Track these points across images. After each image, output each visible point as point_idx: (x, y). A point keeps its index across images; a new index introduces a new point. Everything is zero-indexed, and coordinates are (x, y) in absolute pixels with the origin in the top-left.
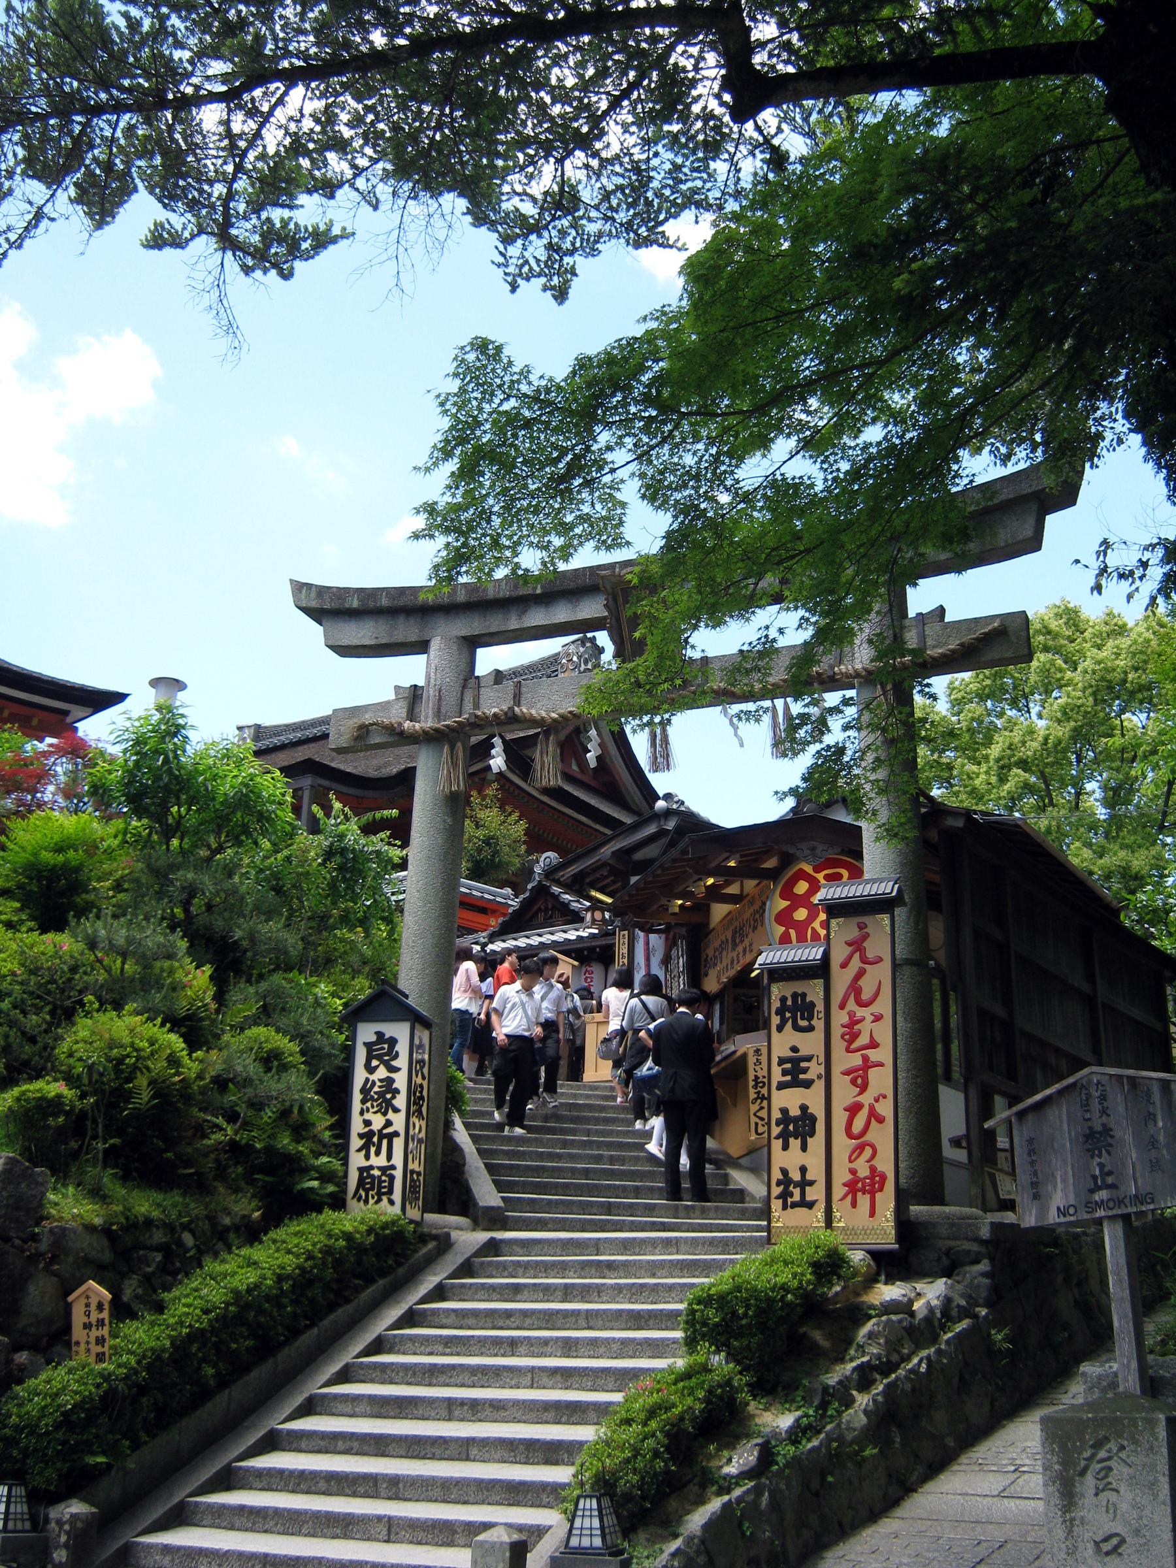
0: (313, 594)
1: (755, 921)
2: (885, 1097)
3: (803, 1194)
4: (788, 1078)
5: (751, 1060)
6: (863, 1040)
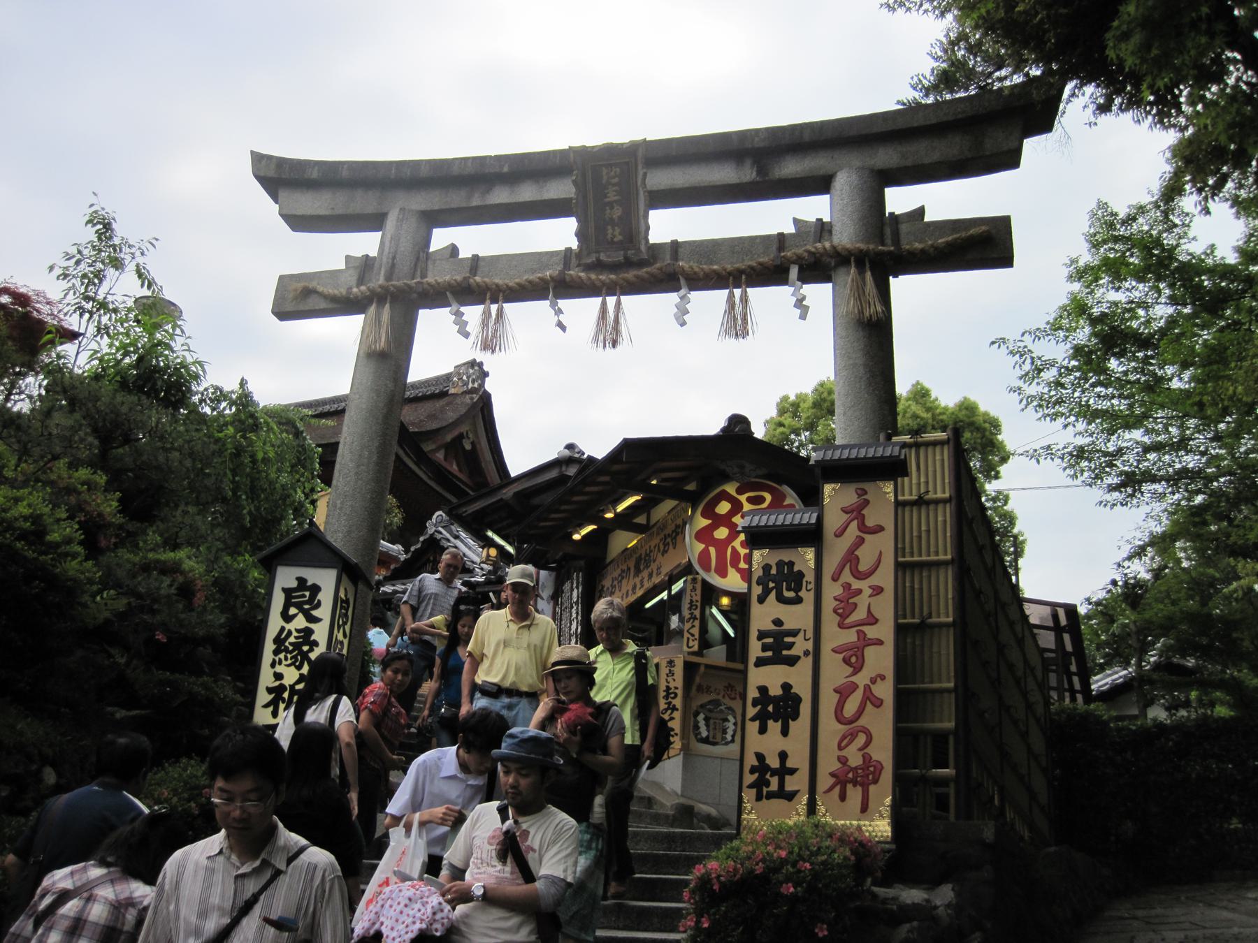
0: (273, 166)
1: (666, 545)
2: (883, 678)
3: (782, 784)
4: (770, 654)
6: (860, 614)
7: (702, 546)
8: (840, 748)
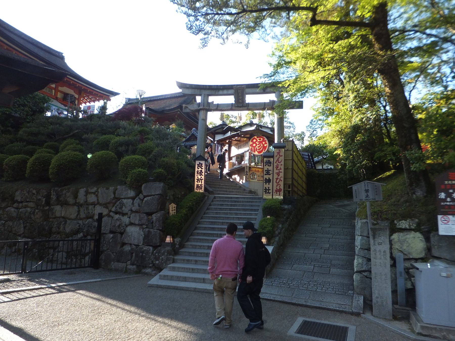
5: (246, 168)
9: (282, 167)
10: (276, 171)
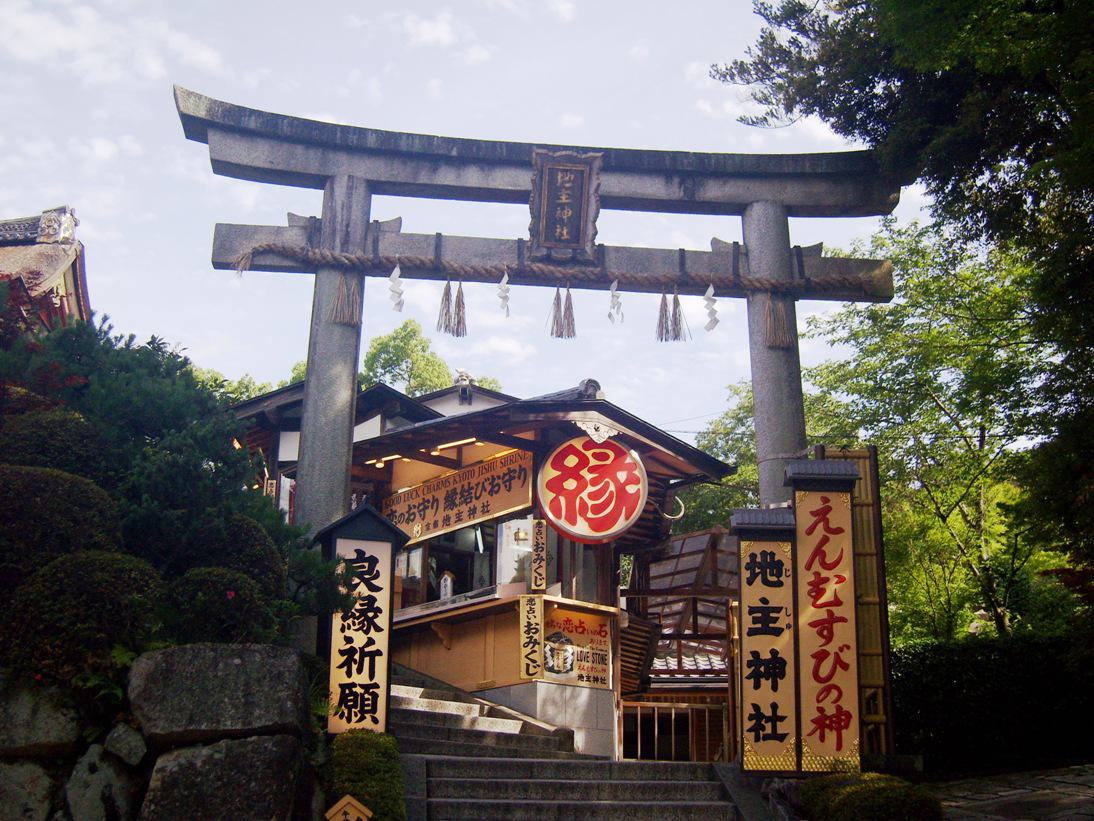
2: (848, 647)
3: (774, 728)
4: (759, 625)
6: (827, 597)
7: (552, 495)
8: (818, 701)
9: (847, 593)
10: (809, 614)
